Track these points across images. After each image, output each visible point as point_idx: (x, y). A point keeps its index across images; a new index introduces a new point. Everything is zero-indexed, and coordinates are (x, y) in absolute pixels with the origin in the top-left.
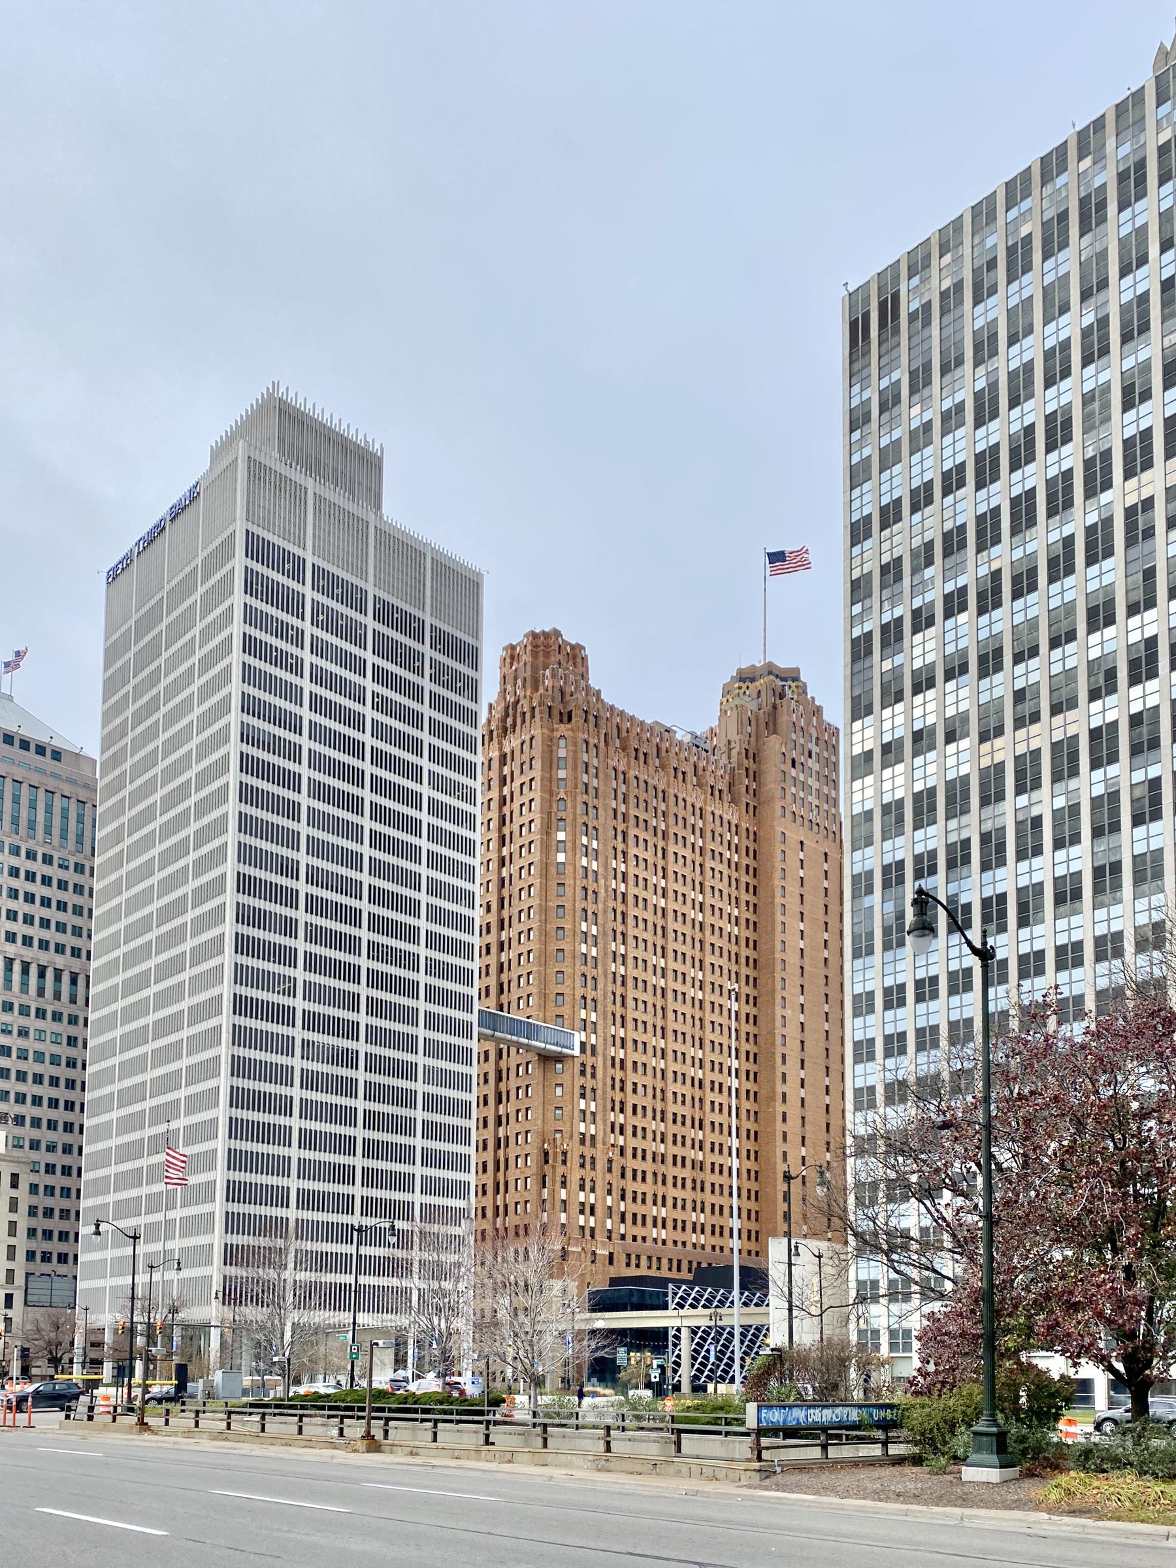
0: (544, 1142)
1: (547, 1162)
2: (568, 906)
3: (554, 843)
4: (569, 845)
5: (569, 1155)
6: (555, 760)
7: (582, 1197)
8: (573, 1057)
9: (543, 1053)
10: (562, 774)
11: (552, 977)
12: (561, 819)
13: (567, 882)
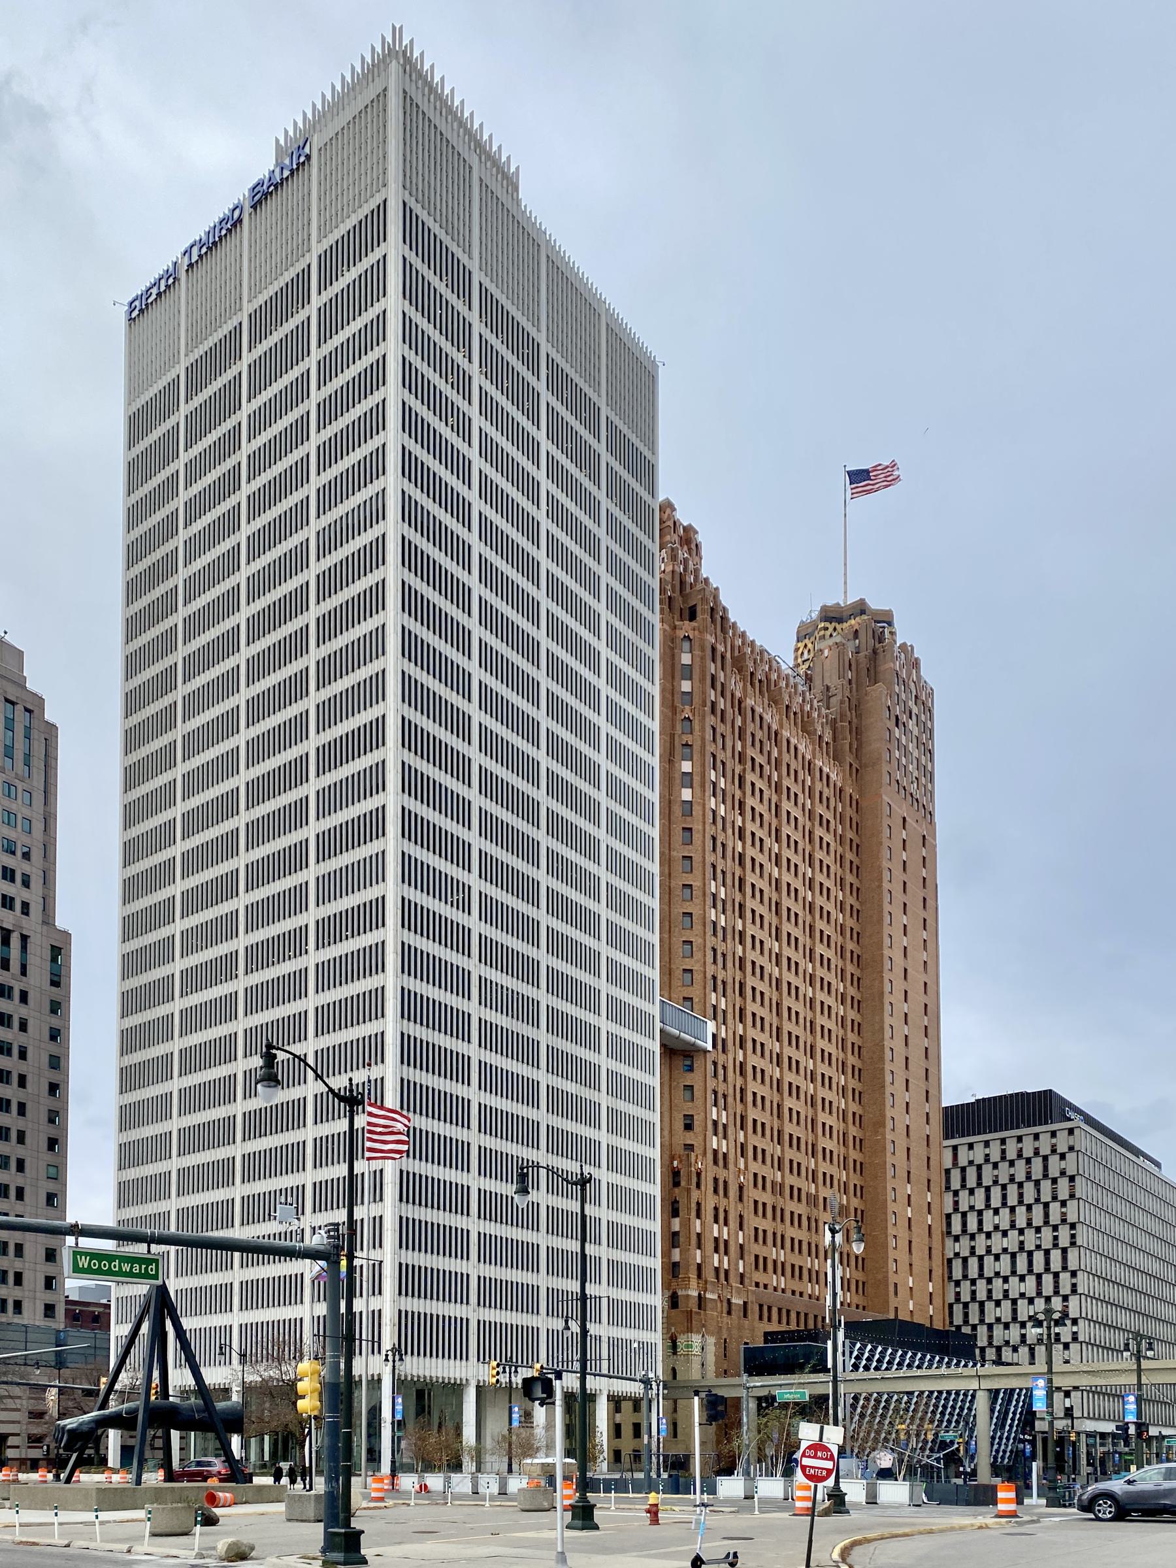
0: (672, 1158)
1: (677, 1184)
2: (697, 858)
3: (677, 776)
4: (697, 779)
5: (703, 1174)
6: (678, 668)
8: (705, 1051)
9: (671, 1045)
10: (686, 686)
11: (678, 949)
12: (686, 745)
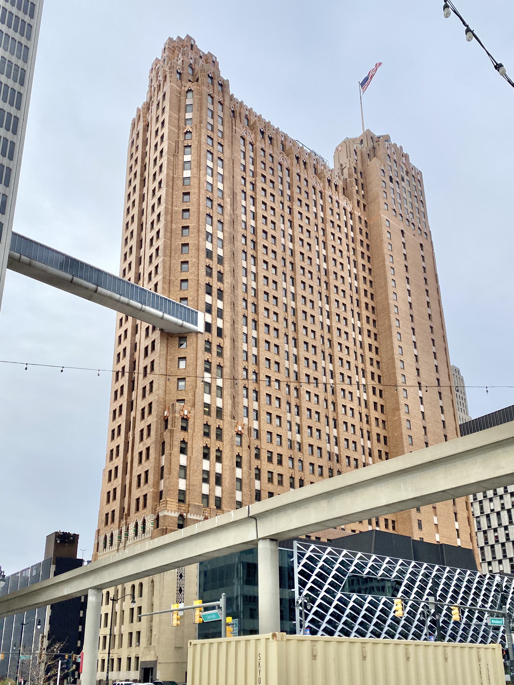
2: (193, 209)
5: (191, 422)
7: (206, 465)
8: (197, 333)
13: (192, 191)
